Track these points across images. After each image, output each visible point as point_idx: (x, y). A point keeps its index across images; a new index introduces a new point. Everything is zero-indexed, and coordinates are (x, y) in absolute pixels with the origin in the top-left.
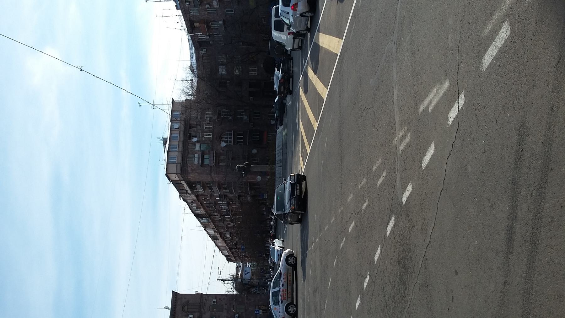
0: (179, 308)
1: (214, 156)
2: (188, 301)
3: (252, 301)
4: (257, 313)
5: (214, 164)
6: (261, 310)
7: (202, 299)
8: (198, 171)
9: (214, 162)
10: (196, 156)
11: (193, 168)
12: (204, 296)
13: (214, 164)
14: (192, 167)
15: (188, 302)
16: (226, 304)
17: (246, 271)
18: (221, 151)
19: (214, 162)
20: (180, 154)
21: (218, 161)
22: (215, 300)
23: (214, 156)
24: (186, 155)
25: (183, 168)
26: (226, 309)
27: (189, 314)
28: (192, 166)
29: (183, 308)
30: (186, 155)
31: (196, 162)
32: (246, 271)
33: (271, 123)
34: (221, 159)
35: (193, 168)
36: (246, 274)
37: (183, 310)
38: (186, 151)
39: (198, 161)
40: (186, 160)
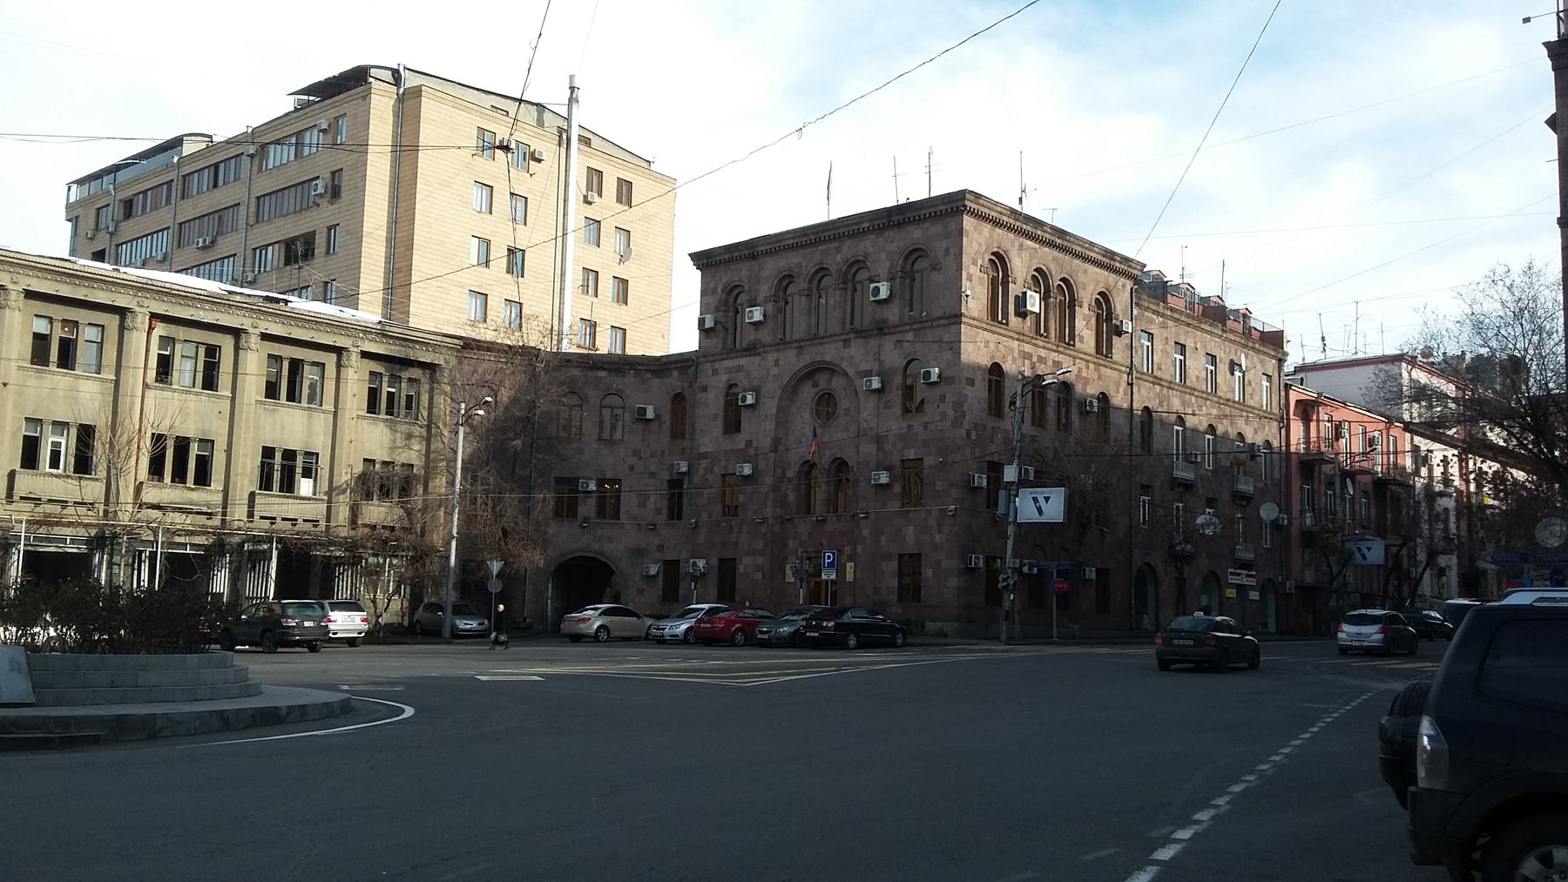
0: (916, 234)
2: (936, 267)
3: (938, 539)
4: (827, 561)
6: (833, 577)
7: (942, 322)
12: (954, 328)
15: (934, 269)
16: (926, 426)
17: (1047, 499)
22: (934, 378)
26: (910, 427)
27: (898, 280)
29: (915, 254)
32: (1047, 499)
36: (1035, 500)
37: (914, 256)
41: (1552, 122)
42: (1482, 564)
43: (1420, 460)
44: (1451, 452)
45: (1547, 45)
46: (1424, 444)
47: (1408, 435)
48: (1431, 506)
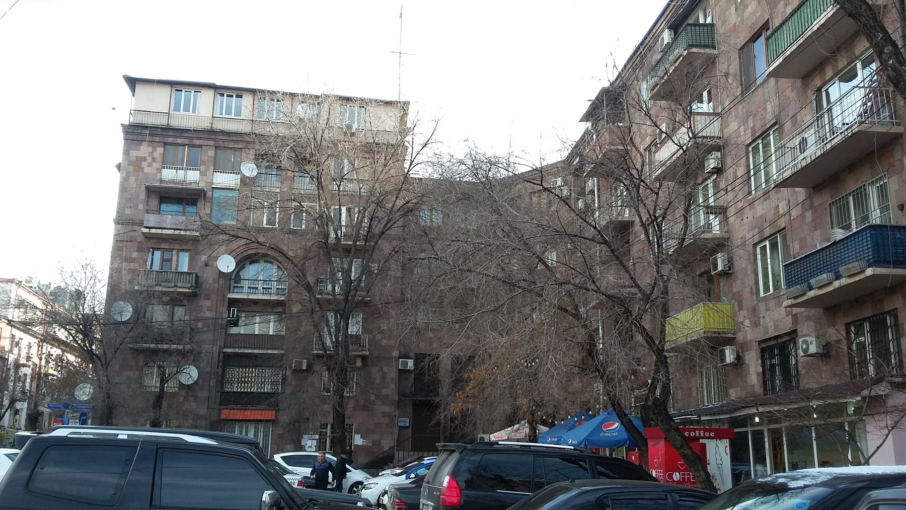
1: (177, 232)
5: (146, 230)
8: (132, 179)
9: (153, 231)
10: (193, 176)
11: (144, 164)
13: (146, 230)
14: (149, 159)
18: (204, 258)
19: (153, 231)
20: (205, 125)
21: (164, 246)
23: (177, 232)
24: (197, 142)
25: (145, 131)
28: (154, 160)
30: (197, 142)
31: (168, 174)
33: (305, 436)
34: (175, 258)
35: (144, 164)
38: (212, 143)
39: (173, 181)
40: (180, 141)
41: (119, 167)
42: (41, 409)
43: (14, 343)
44: (34, 341)
45: (123, 125)
46: (18, 334)
47: (9, 328)
48: (16, 372)
